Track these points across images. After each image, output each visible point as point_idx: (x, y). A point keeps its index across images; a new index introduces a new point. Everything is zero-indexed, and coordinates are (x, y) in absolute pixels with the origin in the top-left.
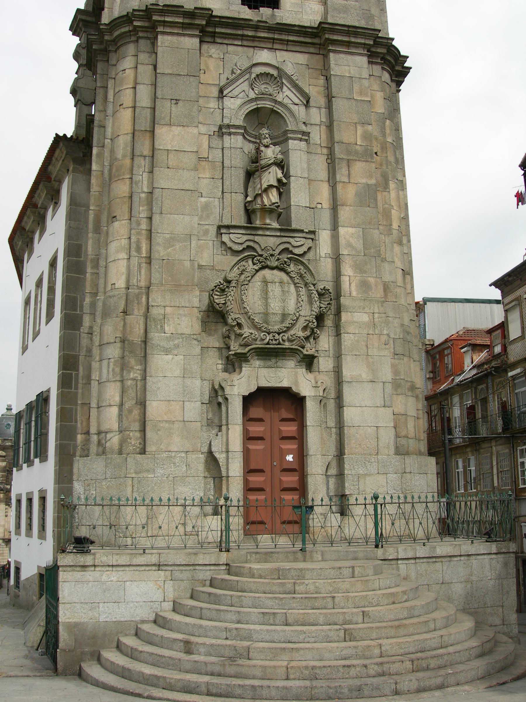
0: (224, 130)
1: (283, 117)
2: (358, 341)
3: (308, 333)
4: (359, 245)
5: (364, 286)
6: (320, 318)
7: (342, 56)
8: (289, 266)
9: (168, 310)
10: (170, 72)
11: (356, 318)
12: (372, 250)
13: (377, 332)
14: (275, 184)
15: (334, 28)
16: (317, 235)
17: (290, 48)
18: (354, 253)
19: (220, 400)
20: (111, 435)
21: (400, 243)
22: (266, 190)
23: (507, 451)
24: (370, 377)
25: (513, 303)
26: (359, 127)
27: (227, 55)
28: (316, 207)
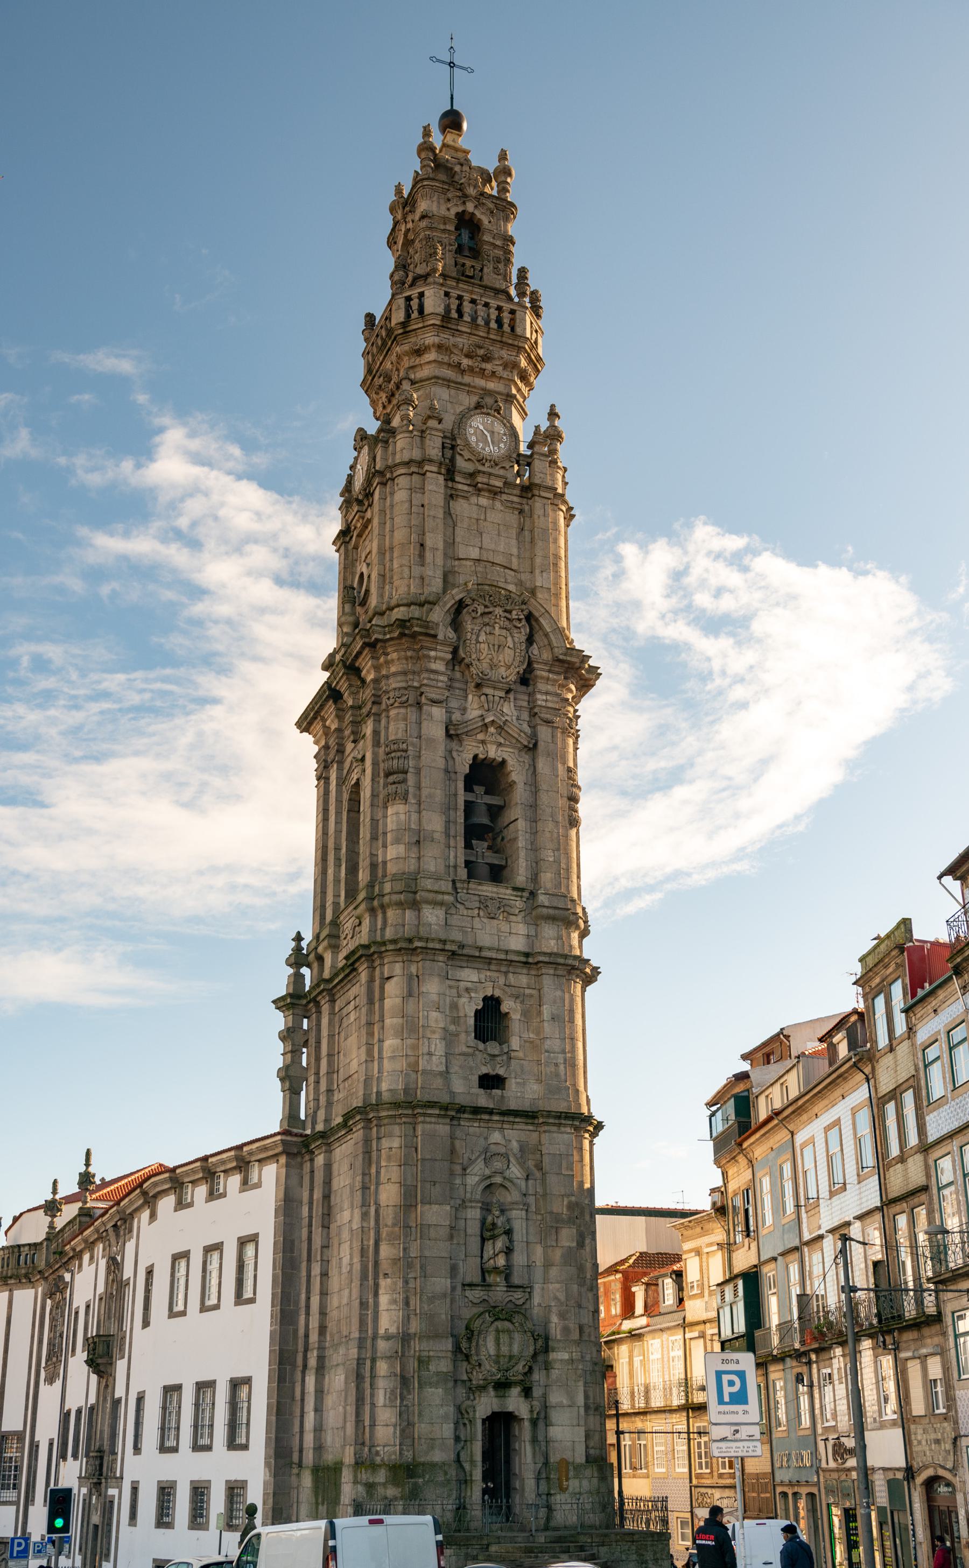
4: (562, 1297)
5: (566, 1330)
6: (535, 1356)
7: (555, 1135)
9: (431, 1354)
10: (429, 1157)
11: (560, 1356)
15: (549, 1114)
17: (515, 1126)
21: (591, 1290)
24: (570, 1403)
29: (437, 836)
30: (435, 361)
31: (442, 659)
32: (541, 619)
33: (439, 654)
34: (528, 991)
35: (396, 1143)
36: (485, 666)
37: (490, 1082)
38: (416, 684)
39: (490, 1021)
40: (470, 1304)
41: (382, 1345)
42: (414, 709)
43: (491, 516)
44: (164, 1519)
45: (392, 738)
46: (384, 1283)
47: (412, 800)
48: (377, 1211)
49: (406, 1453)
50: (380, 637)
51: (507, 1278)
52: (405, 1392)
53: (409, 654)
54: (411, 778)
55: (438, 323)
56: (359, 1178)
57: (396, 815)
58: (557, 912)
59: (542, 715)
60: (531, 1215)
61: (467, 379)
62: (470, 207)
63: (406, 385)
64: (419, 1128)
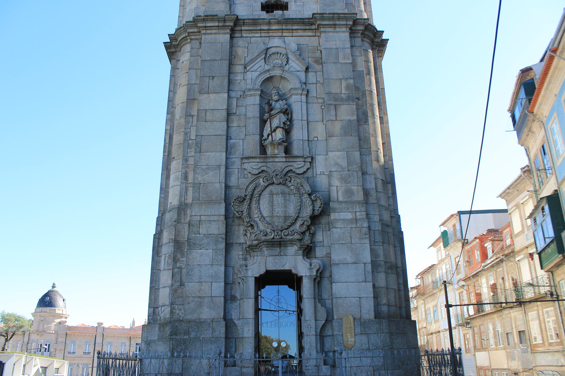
0: (246, 93)
1: (288, 81)
2: (344, 233)
3: (304, 228)
4: (344, 163)
5: (349, 192)
6: (314, 219)
7: (331, 34)
8: (290, 181)
9: (203, 218)
10: (209, 59)
12: (355, 167)
13: (358, 225)
14: (282, 126)
15: (322, 16)
16: (314, 160)
17: (295, 34)
18: (340, 169)
19: (240, 281)
20: (164, 308)
22: (275, 130)
23: (521, 316)
25: (514, 208)
26: (343, 82)
27: (250, 45)
28: (313, 140)
40: (249, 175)
49: (177, 312)
51: (287, 151)
52: (179, 255)
60: (310, 100)
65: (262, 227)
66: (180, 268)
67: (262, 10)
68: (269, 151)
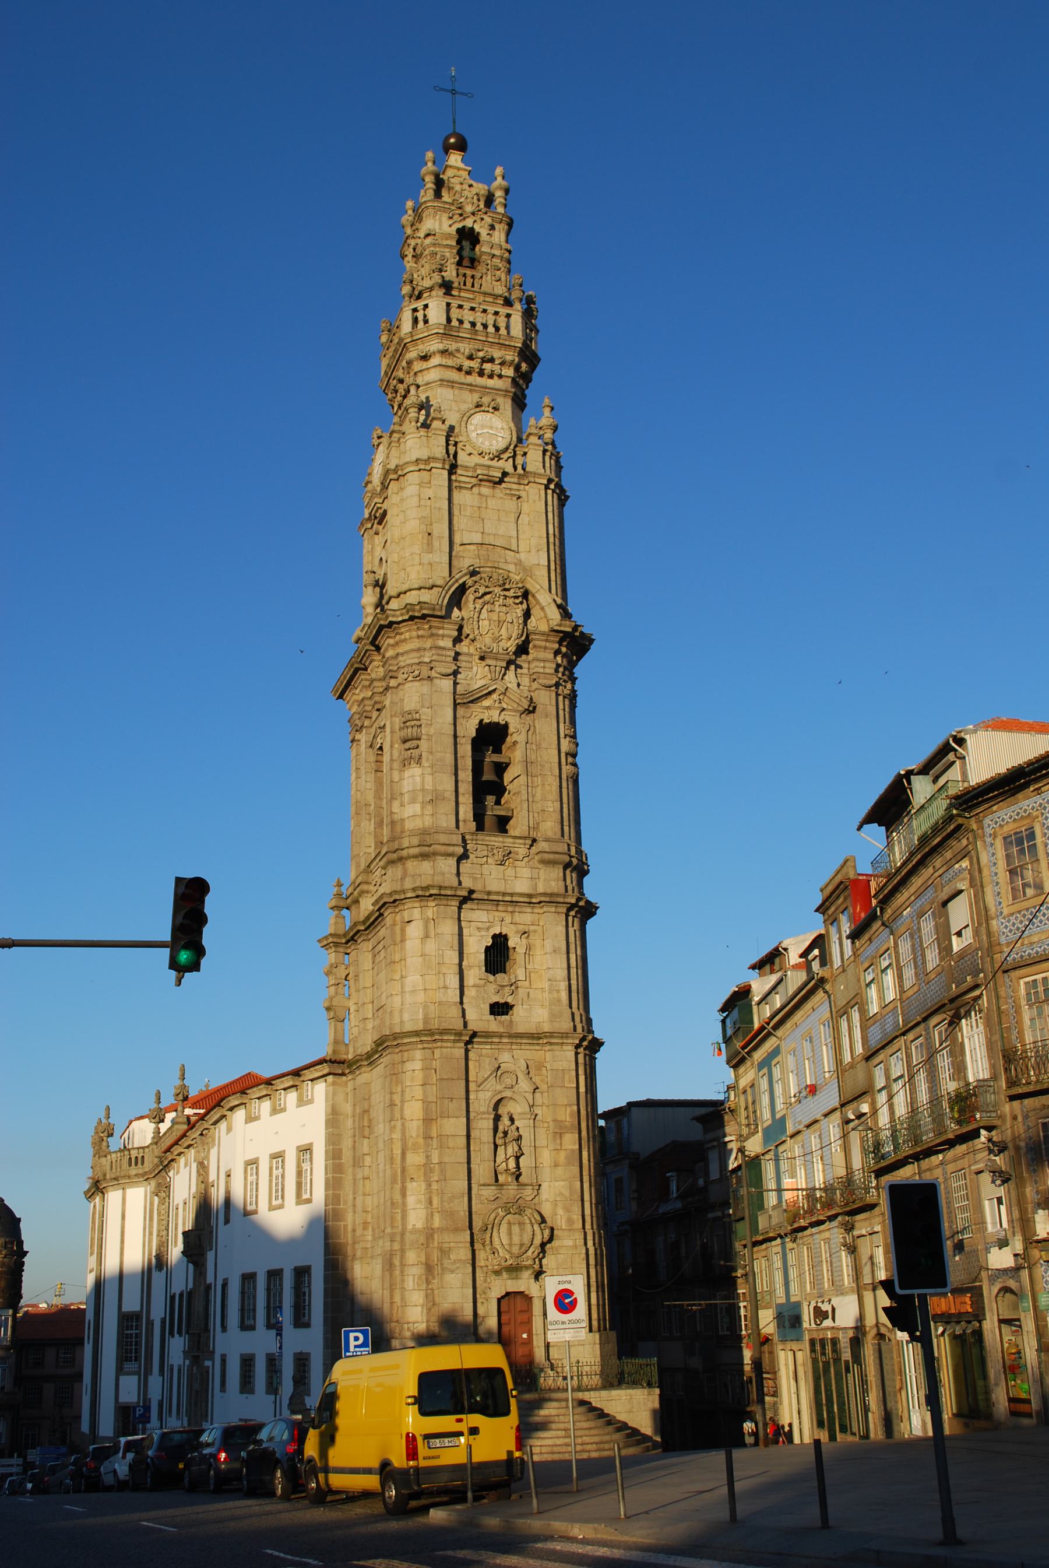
4: (567, 1193)
5: (570, 1221)
6: (543, 1245)
7: (557, 1053)
9: (452, 1245)
10: (446, 1077)
15: (551, 1035)
29: (447, 795)
30: (440, 365)
31: (449, 636)
32: (537, 595)
33: (446, 632)
34: (532, 928)
35: (417, 1065)
36: (488, 640)
37: (499, 1009)
38: (427, 660)
39: (498, 955)
41: (409, 1237)
42: (425, 682)
43: (492, 503)
44: (247, 1384)
45: (407, 709)
46: (411, 1186)
47: (425, 763)
48: (403, 1125)
50: (394, 619)
53: (421, 633)
54: (424, 744)
55: (442, 331)
56: (388, 1097)
57: (413, 778)
58: (557, 856)
59: (540, 681)
61: (469, 379)
62: (469, 223)
63: (413, 390)
64: (437, 1052)
65: (501, 1254)
66: (432, 1289)
67: (491, 1014)
68: (502, 1178)
